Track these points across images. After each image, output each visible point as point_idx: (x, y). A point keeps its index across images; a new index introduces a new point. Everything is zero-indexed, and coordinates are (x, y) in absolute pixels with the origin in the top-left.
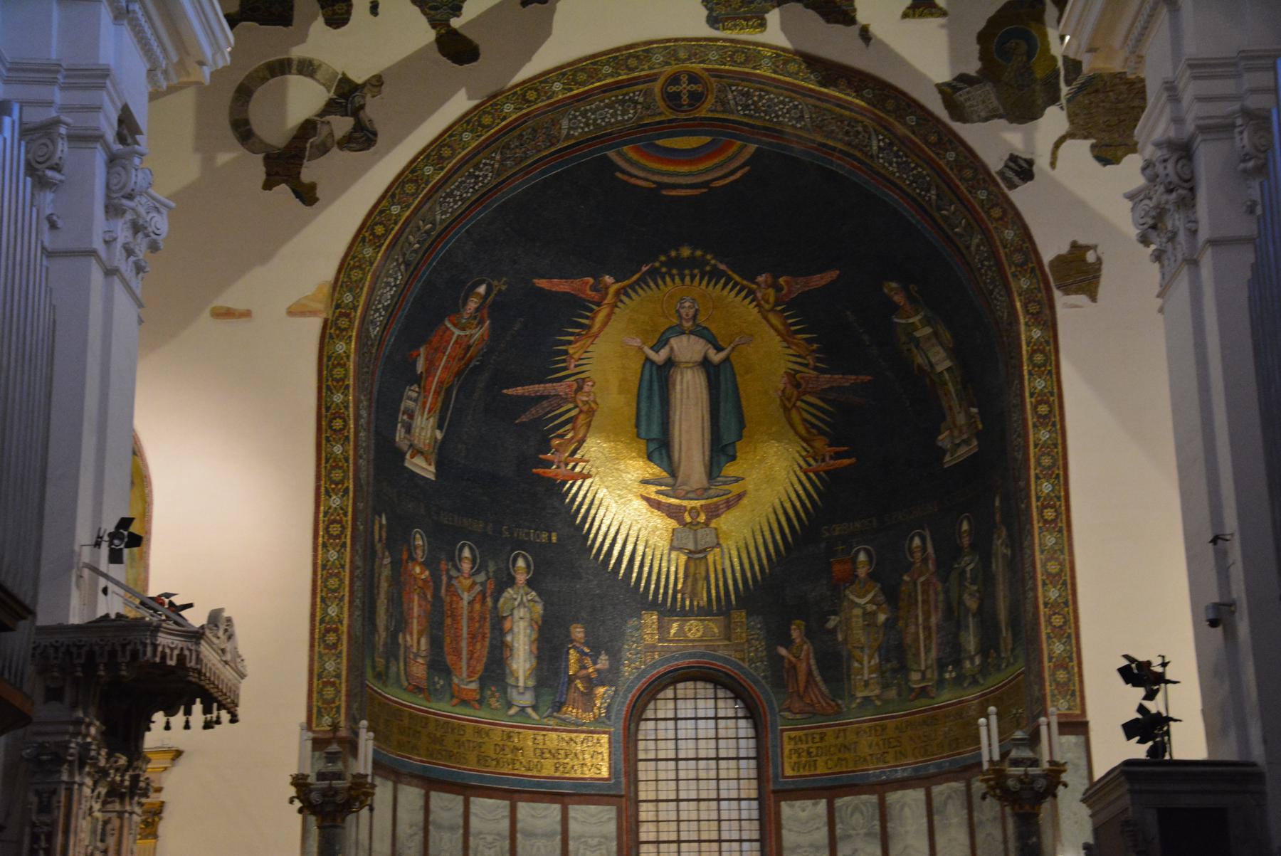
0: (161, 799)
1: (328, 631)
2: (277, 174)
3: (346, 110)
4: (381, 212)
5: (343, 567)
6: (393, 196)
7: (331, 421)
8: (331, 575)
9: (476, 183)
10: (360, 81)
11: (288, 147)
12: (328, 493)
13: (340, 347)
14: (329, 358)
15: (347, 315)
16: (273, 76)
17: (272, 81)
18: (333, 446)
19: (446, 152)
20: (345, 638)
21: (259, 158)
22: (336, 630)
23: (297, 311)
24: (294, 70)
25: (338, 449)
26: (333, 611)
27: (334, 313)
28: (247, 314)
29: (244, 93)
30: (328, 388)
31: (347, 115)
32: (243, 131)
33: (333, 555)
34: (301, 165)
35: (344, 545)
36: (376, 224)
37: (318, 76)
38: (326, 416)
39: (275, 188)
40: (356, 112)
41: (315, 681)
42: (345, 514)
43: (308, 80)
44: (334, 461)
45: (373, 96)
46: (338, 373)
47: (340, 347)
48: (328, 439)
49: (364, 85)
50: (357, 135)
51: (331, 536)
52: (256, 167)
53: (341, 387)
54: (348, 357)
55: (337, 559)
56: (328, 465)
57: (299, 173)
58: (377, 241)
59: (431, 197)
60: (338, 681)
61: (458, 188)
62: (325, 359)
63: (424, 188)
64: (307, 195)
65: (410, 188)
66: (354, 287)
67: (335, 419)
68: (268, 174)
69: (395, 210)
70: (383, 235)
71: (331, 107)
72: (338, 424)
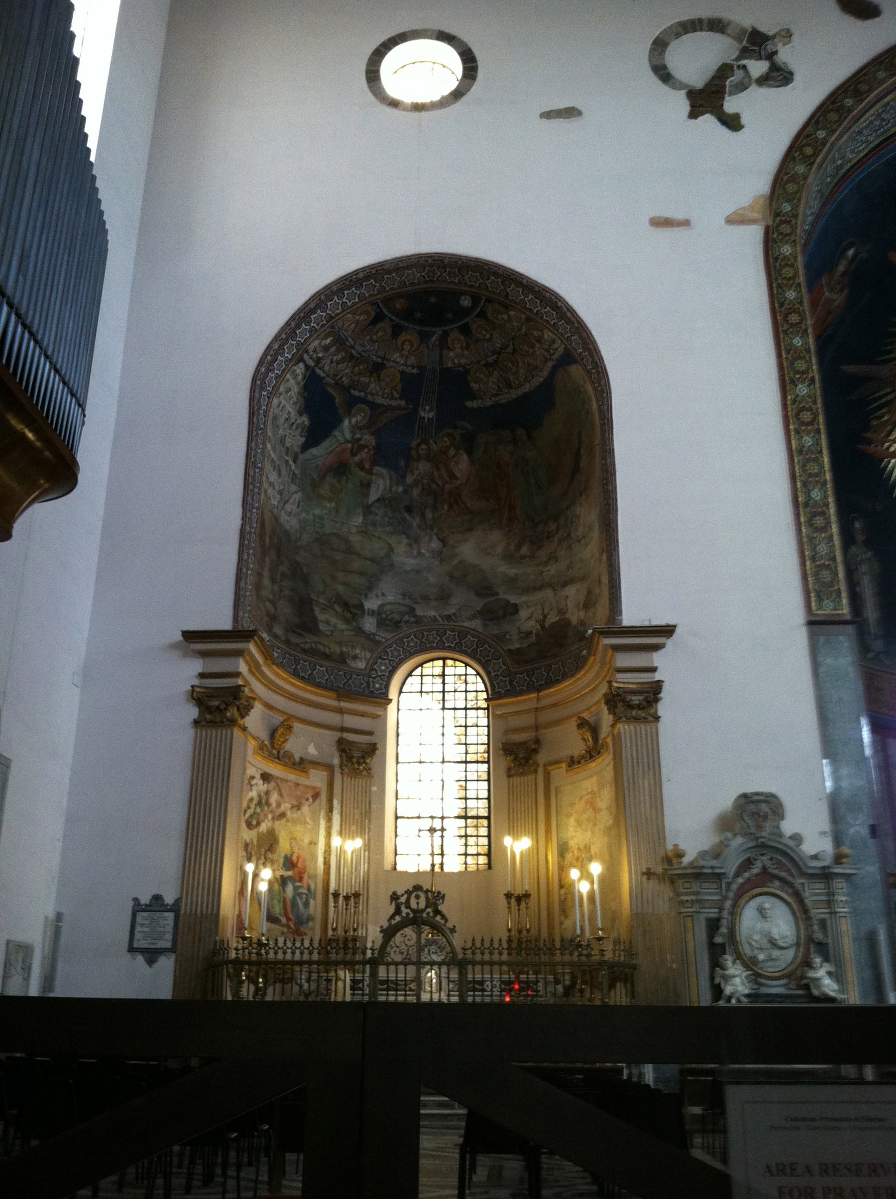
0: (657, 679)
1: (815, 515)
2: (701, 106)
3: (760, 55)
4: (808, 136)
5: (821, 452)
6: (817, 122)
7: (786, 316)
8: (808, 460)
9: (881, 126)
10: (771, 33)
11: (709, 85)
12: (793, 382)
13: (786, 250)
14: (776, 259)
15: (789, 222)
16: (686, 33)
17: (684, 37)
18: (791, 339)
19: (864, 87)
20: (833, 519)
21: (682, 94)
22: (823, 514)
23: (735, 220)
24: (705, 27)
25: (798, 342)
26: (816, 494)
27: (774, 221)
28: (686, 223)
29: (660, 45)
30: (779, 286)
31: (761, 59)
32: (663, 74)
33: (808, 441)
34: (724, 98)
35: (818, 431)
36: (804, 146)
37: (729, 31)
38: (780, 312)
39: (699, 118)
40: (770, 56)
41: (808, 563)
42: (815, 402)
43: (718, 36)
44: (795, 353)
45: (785, 45)
46: (788, 272)
47: (786, 250)
48: (785, 332)
49: (774, 36)
50: (775, 74)
51: (803, 423)
52: (681, 103)
53: (791, 286)
54: (795, 258)
55: (813, 445)
56: (790, 356)
57: (722, 105)
58: (809, 161)
59: (850, 128)
60: (833, 566)
61: (868, 126)
62: (771, 260)
63: (846, 118)
64: (733, 123)
65: (833, 116)
66: (794, 198)
67: (790, 314)
68: (692, 106)
69: (821, 134)
70: (812, 156)
71: (745, 53)
72: (794, 318)
